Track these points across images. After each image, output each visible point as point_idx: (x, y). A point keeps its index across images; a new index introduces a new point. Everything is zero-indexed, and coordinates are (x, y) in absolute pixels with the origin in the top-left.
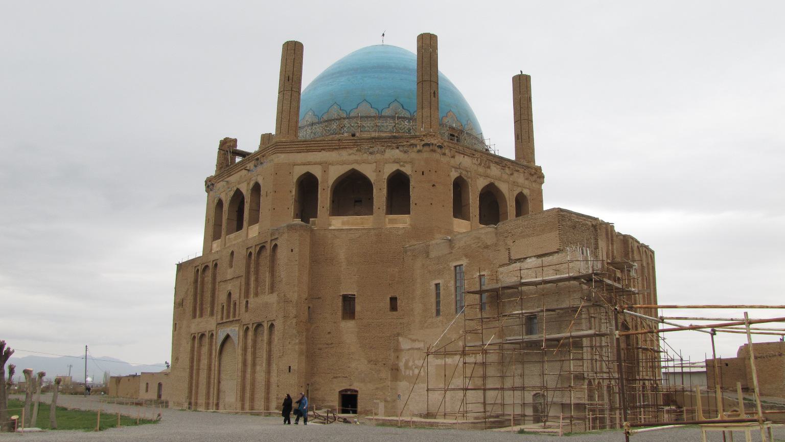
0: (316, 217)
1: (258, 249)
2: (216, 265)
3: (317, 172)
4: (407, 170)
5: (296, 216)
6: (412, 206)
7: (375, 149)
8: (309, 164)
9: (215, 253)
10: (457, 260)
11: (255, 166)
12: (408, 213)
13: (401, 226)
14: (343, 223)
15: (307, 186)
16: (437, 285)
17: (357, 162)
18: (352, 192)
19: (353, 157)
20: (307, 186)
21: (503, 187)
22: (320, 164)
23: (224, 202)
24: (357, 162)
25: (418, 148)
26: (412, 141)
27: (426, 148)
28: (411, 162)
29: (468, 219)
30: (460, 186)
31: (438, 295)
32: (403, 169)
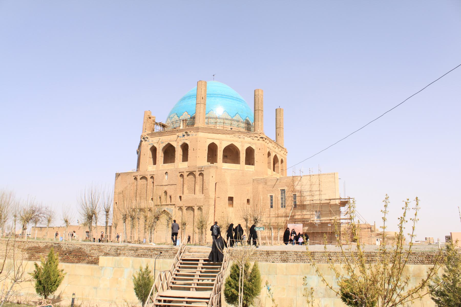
0: (216, 162)
1: (188, 173)
2: (152, 177)
3: (217, 142)
4: (253, 147)
5: (208, 161)
6: (255, 162)
7: (241, 136)
9: (152, 171)
10: (282, 187)
12: (253, 164)
13: (251, 170)
16: (271, 197)
17: (233, 141)
18: (231, 154)
19: (232, 139)
20: (212, 149)
21: (278, 156)
24: (233, 141)
25: (259, 138)
26: (256, 135)
27: (261, 139)
29: (270, 169)
30: (269, 154)
31: (272, 200)
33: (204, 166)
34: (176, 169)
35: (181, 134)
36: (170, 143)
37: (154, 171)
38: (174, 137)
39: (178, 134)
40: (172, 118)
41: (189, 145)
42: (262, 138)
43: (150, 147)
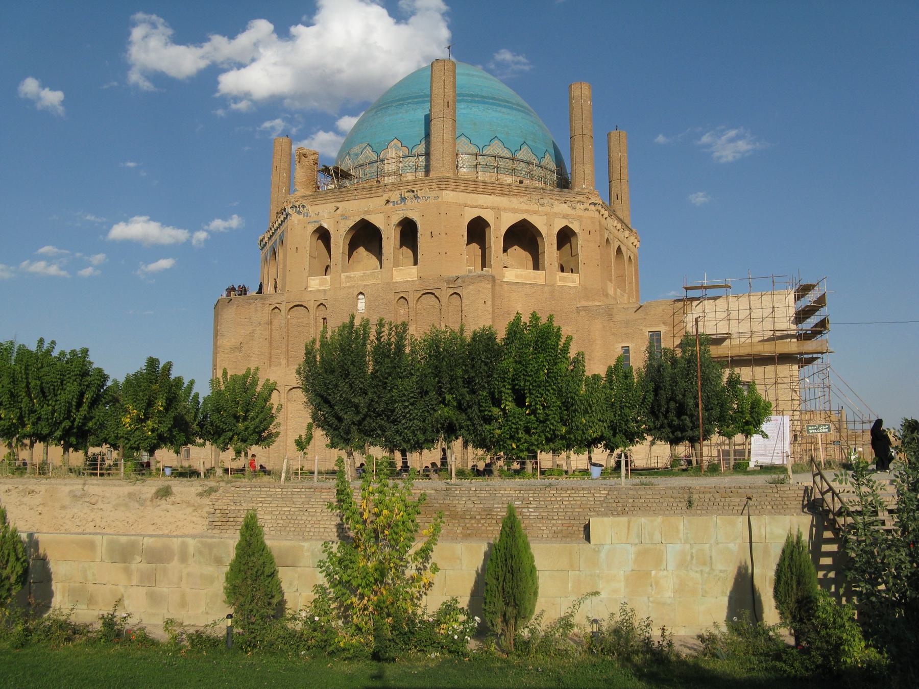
3: (488, 216)
4: (575, 227)
7: (545, 201)
8: (480, 207)
9: (319, 291)
10: (651, 325)
11: (403, 199)
14: (517, 276)
15: (477, 231)
19: (524, 207)
20: (477, 231)
21: (623, 249)
22: (492, 209)
23: (332, 232)
24: (527, 211)
25: (586, 206)
28: (580, 218)
32: (570, 225)
33: (463, 278)
34: (388, 284)
35: (395, 196)
36: (367, 218)
37: (325, 291)
38: (379, 202)
39: (386, 197)
40: (357, 155)
41: (419, 224)
42: (595, 204)
43: (312, 228)
